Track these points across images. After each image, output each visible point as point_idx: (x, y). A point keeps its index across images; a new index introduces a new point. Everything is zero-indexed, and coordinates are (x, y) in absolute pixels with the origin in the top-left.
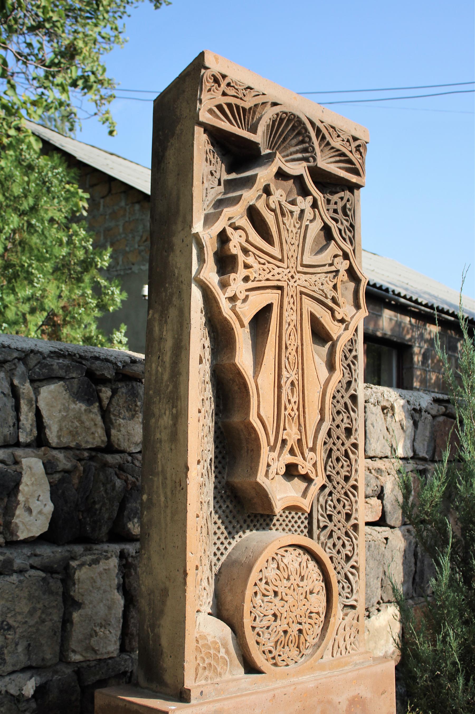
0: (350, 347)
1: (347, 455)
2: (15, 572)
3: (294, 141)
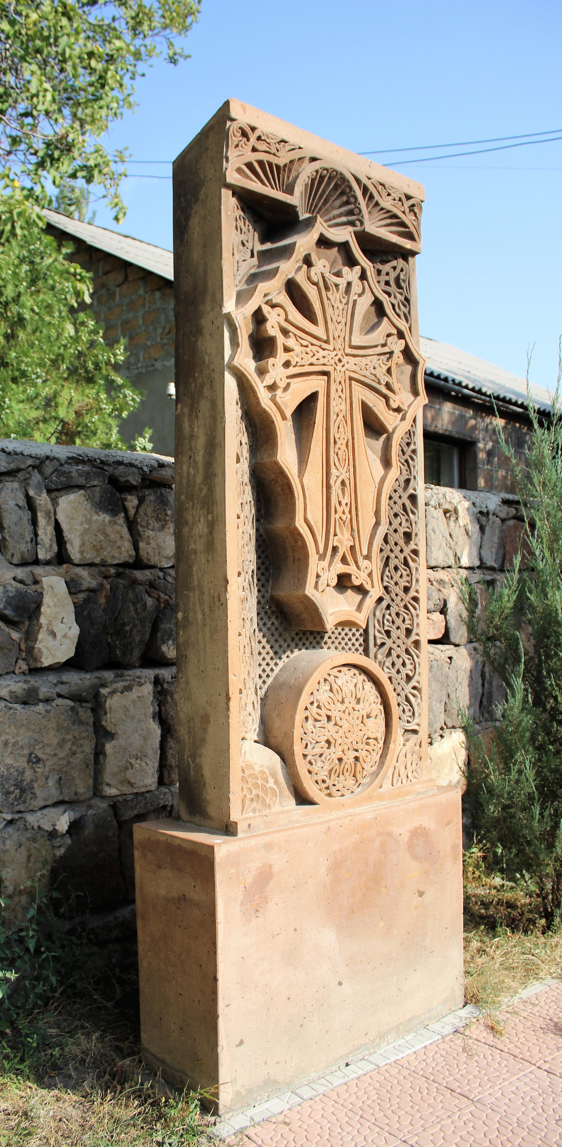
0: (407, 440)
1: (406, 563)
3: (338, 203)
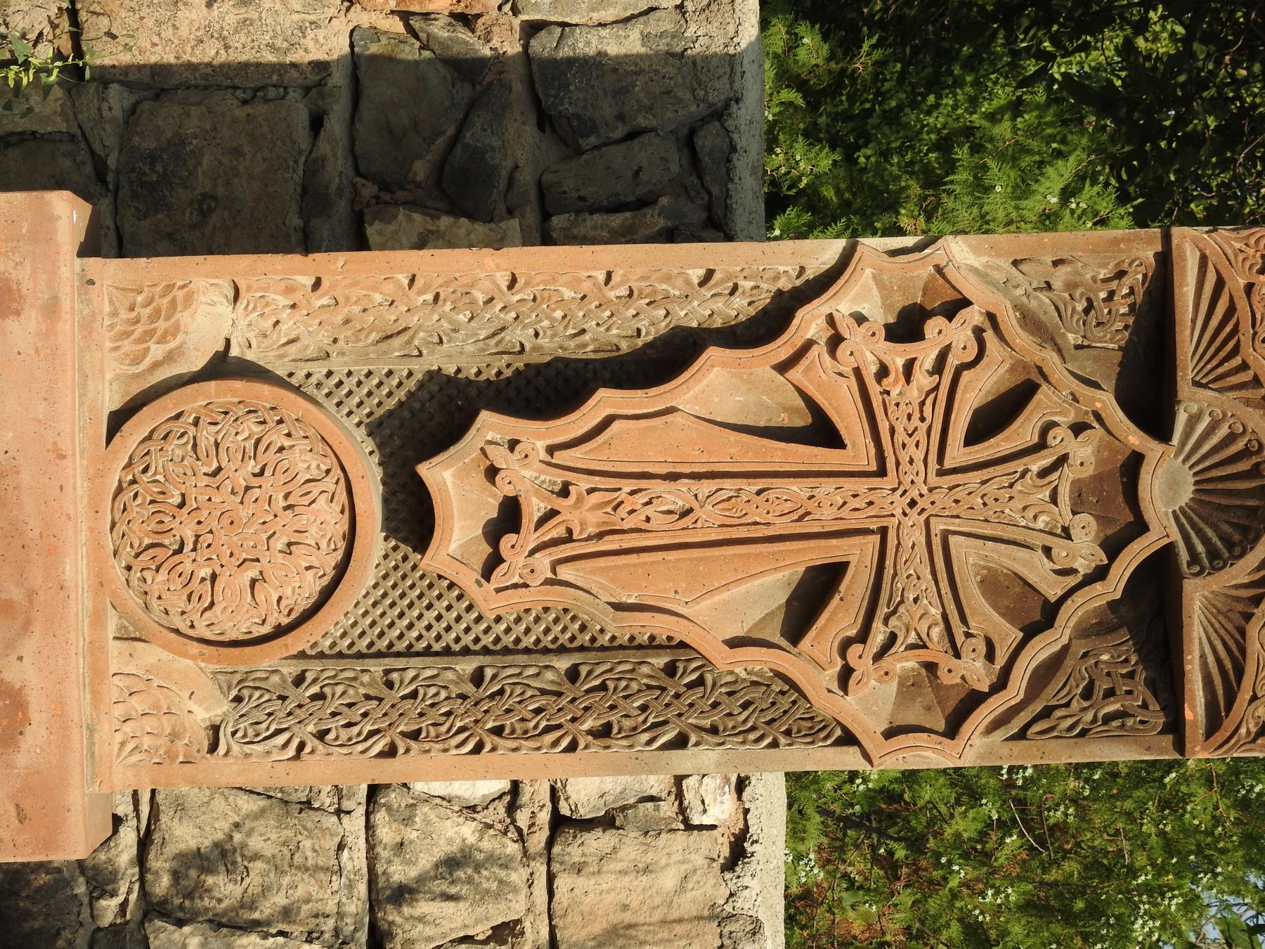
0: (795, 729)
1: (548, 729)
2: (307, 223)
3: (1226, 528)
